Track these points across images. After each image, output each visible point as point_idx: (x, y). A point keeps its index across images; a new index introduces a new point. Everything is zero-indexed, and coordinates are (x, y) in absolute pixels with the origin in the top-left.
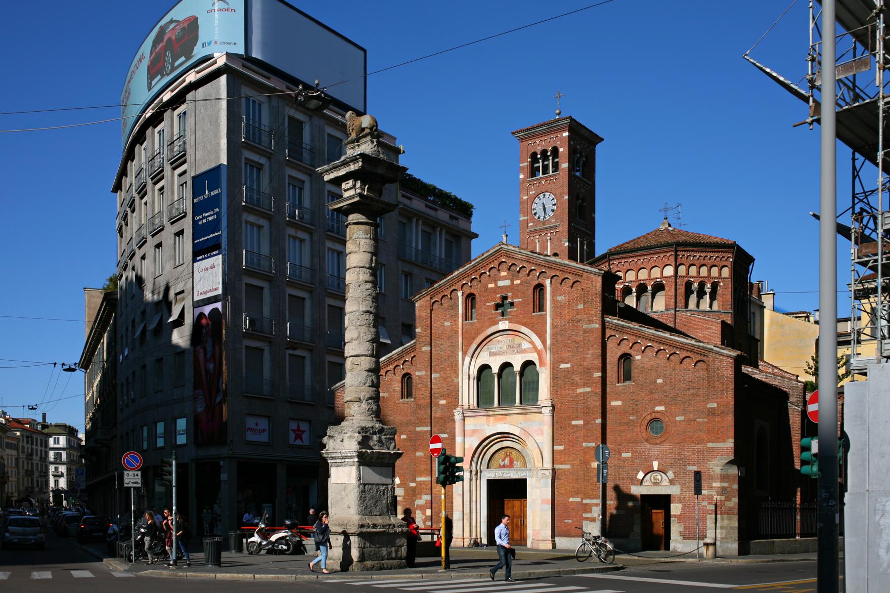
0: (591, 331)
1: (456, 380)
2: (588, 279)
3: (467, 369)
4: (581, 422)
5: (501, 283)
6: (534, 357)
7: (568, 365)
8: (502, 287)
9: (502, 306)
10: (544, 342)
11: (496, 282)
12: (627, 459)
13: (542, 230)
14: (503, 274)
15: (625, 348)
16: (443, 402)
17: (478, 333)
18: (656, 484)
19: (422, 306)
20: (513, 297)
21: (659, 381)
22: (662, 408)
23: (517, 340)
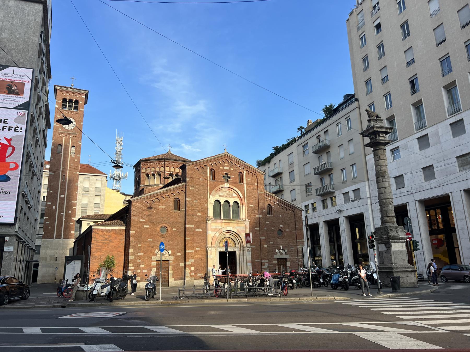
0: (261, 194)
1: (206, 205)
2: (259, 175)
3: (211, 200)
4: (259, 229)
5: (225, 168)
6: (238, 200)
7: (253, 206)
8: (226, 170)
9: (227, 177)
10: (243, 195)
11: (223, 167)
12: (272, 244)
13: (67, 134)
14: (226, 164)
15: (269, 202)
16: (200, 214)
17: (216, 186)
18: (281, 254)
19: (190, 169)
20: (230, 175)
21: (280, 216)
22: (281, 226)
23: (231, 192)
